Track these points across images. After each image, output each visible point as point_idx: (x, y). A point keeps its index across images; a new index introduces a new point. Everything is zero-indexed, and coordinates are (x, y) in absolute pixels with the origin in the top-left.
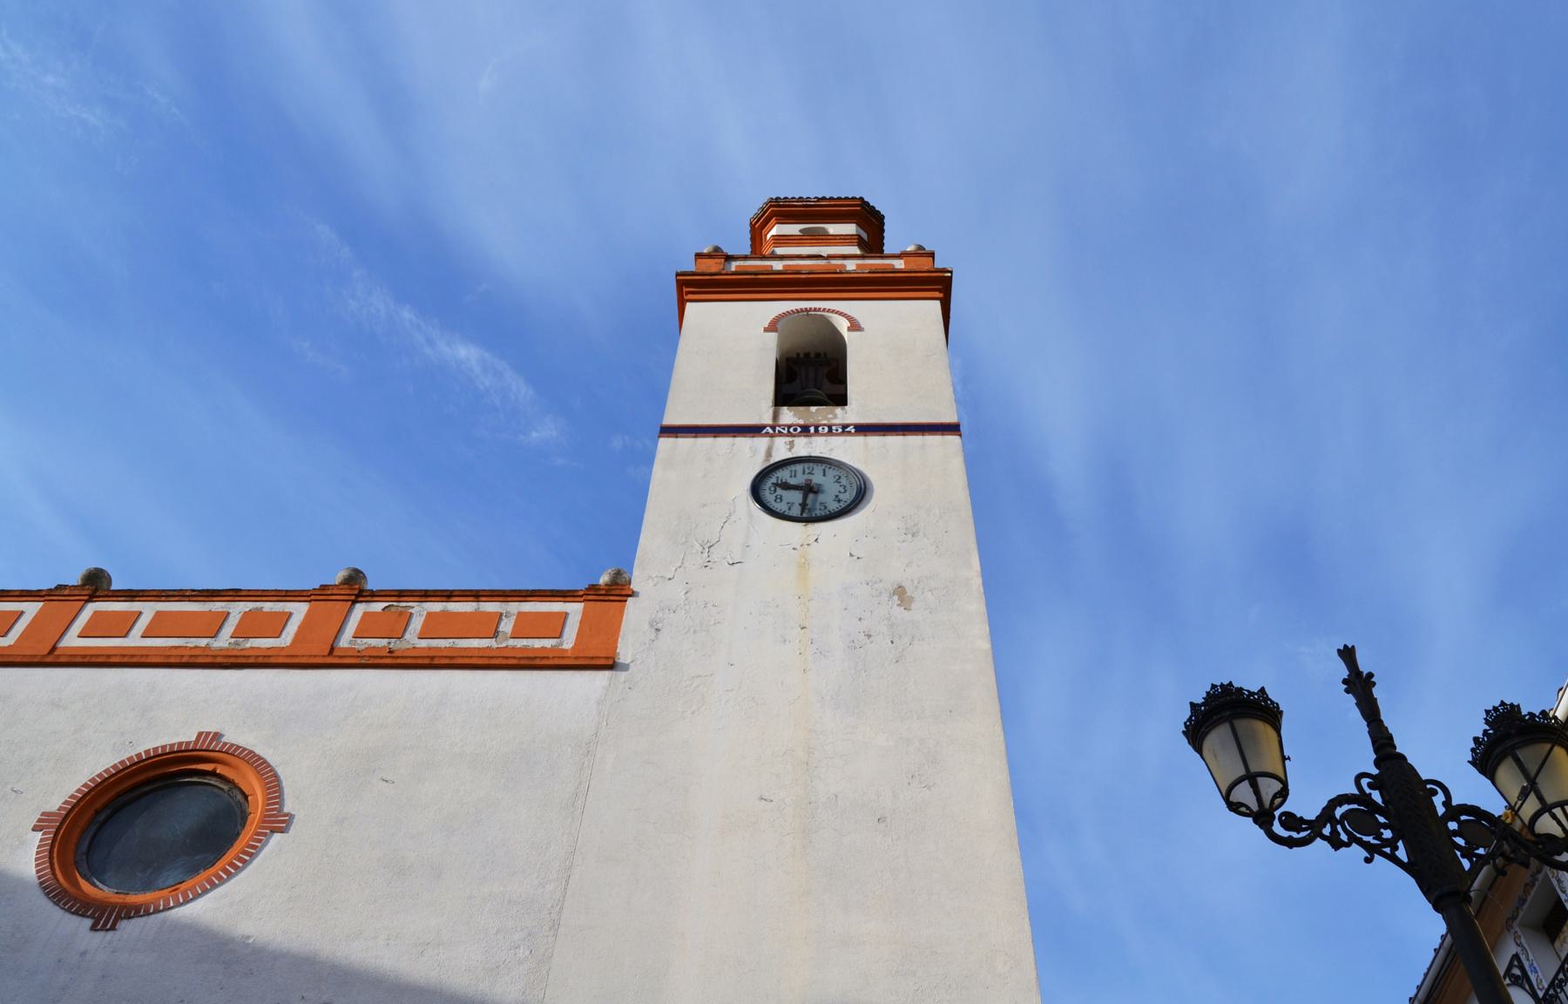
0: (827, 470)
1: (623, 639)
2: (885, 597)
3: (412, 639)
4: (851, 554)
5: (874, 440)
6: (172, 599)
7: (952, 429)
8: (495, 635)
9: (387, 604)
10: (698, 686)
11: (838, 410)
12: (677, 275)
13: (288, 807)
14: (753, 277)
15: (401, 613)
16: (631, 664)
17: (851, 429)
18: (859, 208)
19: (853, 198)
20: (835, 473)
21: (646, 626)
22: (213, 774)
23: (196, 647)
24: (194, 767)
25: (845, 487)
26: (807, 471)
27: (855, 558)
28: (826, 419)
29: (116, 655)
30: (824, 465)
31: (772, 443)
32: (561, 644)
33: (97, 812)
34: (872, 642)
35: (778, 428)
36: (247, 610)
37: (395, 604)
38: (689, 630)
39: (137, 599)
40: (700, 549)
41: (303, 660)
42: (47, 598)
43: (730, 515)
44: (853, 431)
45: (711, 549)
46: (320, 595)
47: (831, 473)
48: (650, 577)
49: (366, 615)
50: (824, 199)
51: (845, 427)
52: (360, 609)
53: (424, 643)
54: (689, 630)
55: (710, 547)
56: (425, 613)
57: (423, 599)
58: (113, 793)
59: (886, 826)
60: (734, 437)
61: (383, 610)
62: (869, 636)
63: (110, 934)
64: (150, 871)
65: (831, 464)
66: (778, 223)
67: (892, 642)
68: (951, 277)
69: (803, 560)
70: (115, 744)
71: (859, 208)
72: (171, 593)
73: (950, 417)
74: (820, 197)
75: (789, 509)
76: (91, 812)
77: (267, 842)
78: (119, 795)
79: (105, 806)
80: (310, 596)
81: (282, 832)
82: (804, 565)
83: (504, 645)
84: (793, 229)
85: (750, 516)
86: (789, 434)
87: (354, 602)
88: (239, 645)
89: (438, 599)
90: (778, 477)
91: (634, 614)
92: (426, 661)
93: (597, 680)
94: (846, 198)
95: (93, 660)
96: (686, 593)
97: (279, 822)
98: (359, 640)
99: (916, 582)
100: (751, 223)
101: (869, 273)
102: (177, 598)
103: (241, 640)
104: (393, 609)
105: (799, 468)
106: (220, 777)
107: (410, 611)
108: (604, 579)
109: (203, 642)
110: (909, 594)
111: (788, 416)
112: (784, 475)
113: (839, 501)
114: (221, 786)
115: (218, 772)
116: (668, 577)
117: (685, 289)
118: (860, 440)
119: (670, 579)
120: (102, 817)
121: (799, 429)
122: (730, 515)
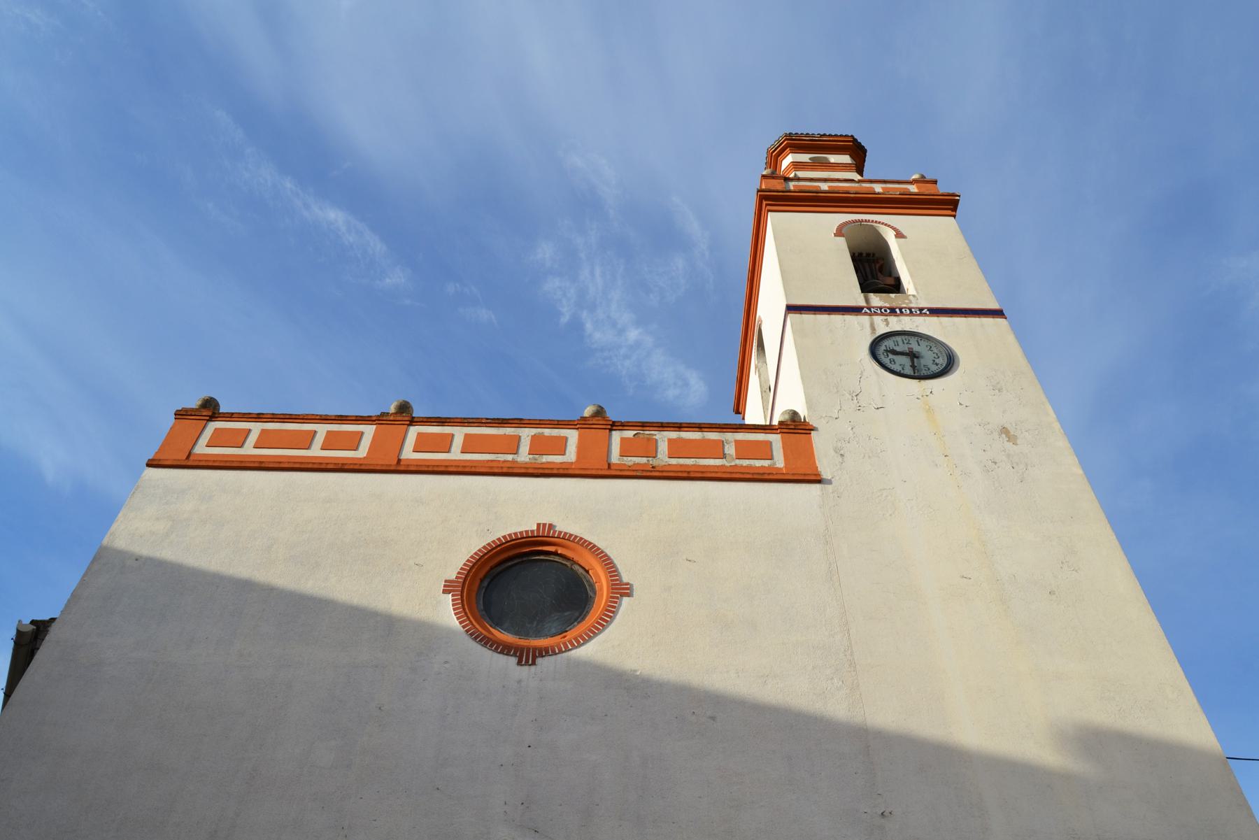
0: (919, 341)
1: (819, 462)
2: (996, 435)
3: (663, 457)
4: (960, 404)
6: (472, 425)
7: (997, 313)
8: (724, 456)
9: (636, 432)
10: (887, 496)
13: (625, 580)
15: (649, 440)
16: (833, 480)
19: (846, 136)
20: (927, 344)
21: (832, 453)
22: (556, 554)
23: (505, 461)
24: (540, 548)
25: (937, 354)
26: (905, 342)
28: (904, 303)
29: (452, 466)
33: (482, 581)
34: (999, 467)
35: (872, 309)
36: (533, 434)
38: (864, 456)
39: (447, 424)
41: (594, 472)
42: (377, 422)
44: (928, 313)
45: (858, 397)
47: (924, 343)
48: (821, 417)
50: (824, 135)
51: (921, 310)
53: (674, 461)
54: (864, 456)
55: (856, 396)
57: (661, 429)
58: (487, 568)
61: (634, 435)
62: (995, 463)
63: (533, 668)
64: (535, 623)
65: (921, 337)
66: (792, 153)
67: (1013, 468)
68: (959, 200)
69: (927, 407)
70: (477, 531)
72: (471, 421)
73: (994, 305)
74: (822, 134)
75: (903, 369)
76: (478, 581)
77: (620, 605)
78: (492, 568)
79: (485, 577)
81: (629, 596)
83: (733, 464)
84: (805, 158)
86: (882, 314)
87: (611, 430)
89: (672, 429)
90: (886, 346)
92: (685, 475)
94: (841, 136)
95: (436, 469)
98: (625, 458)
99: (1014, 425)
102: (476, 425)
103: (537, 456)
104: (641, 436)
105: (899, 339)
106: (561, 556)
107: (654, 437)
108: (588, 412)
109: (510, 457)
112: (889, 343)
113: (937, 364)
114: (563, 562)
115: (559, 552)
119: (836, 418)
120: (485, 584)
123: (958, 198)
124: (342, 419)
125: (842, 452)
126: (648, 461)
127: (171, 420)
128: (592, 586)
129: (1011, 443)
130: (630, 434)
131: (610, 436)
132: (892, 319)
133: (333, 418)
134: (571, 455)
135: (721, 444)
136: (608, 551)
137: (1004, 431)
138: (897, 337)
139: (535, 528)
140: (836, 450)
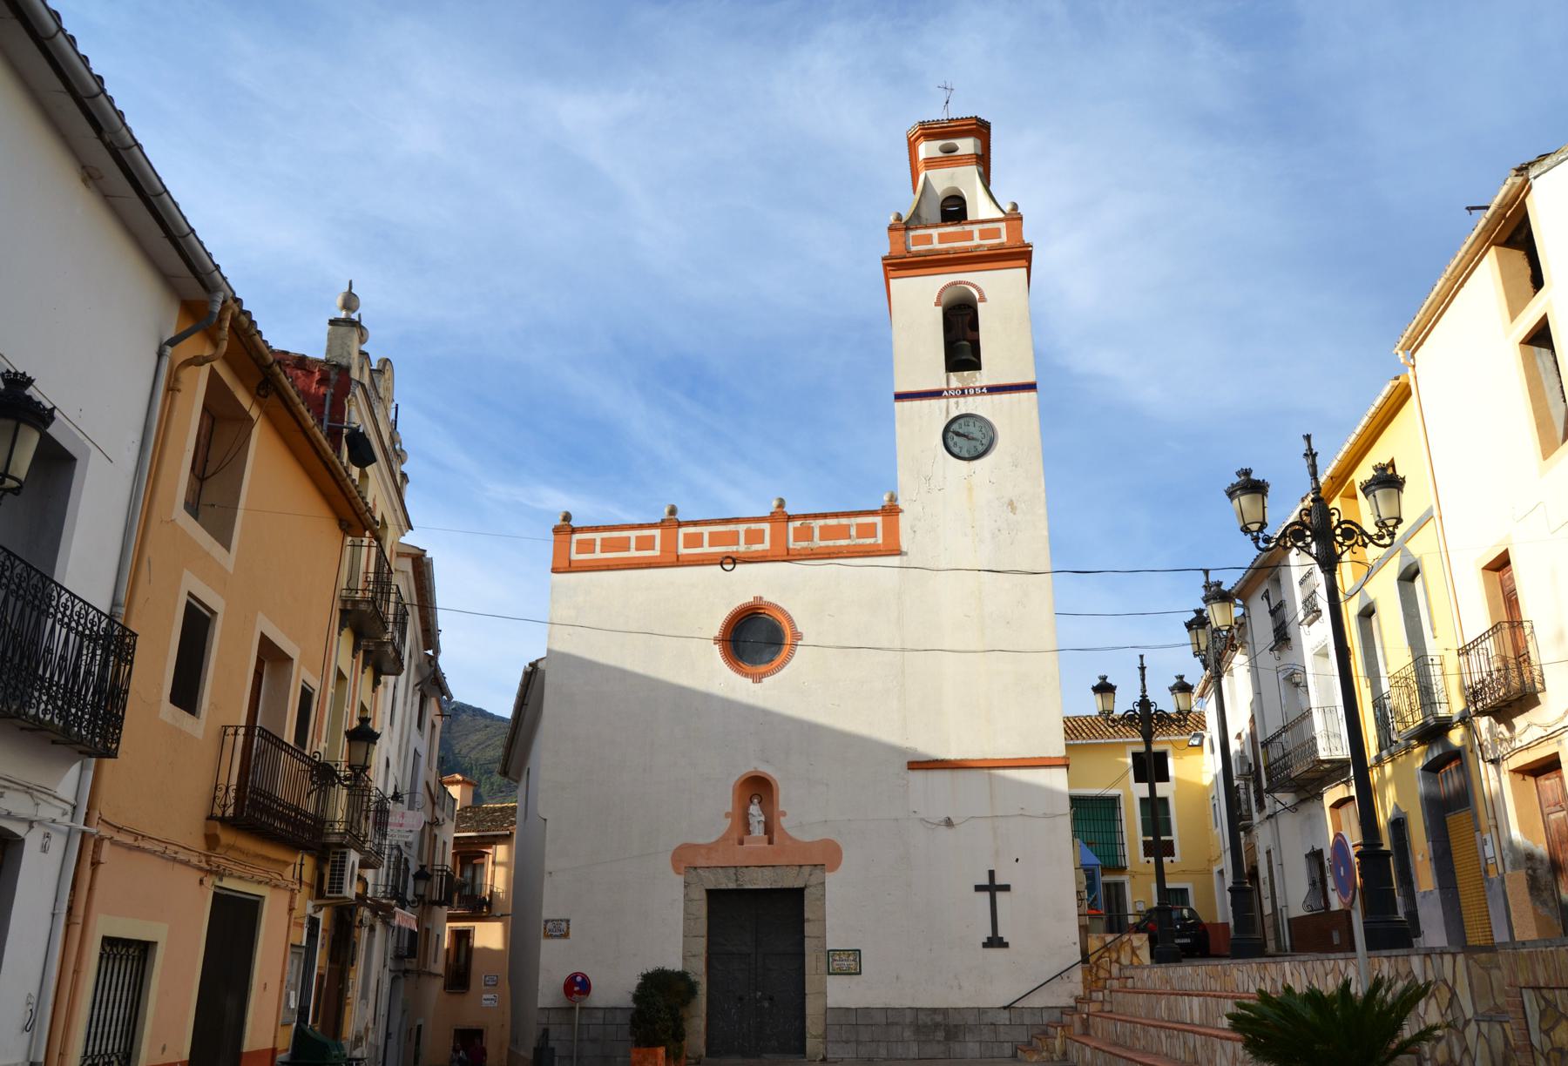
3: (818, 543)
5: (997, 397)
7: (1031, 387)
8: (850, 537)
11: (977, 373)
13: (799, 630)
17: (984, 390)
19: (971, 118)
21: (909, 531)
22: (764, 613)
31: (948, 402)
32: (877, 541)
46: (772, 518)
49: (795, 529)
50: (952, 119)
62: (999, 530)
63: (760, 684)
68: (1031, 251)
78: (737, 623)
82: (970, 489)
83: (854, 543)
86: (956, 396)
87: (787, 521)
91: (904, 520)
93: (895, 560)
97: (798, 636)
100: (909, 139)
106: (768, 615)
109: (734, 548)
111: (956, 380)
112: (955, 427)
117: (888, 268)
118: (989, 398)
123: (1030, 249)
124: (641, 526)
125: (915, 529)
127: (551, 536)
128: (783, 632)
130: (798, 523)
131: (787, 526)
132: (962, 400)
134: (766, 545)
135: (849, 527)
136: (790, 612)
137: (1011, 504)
139: (752, 600)
140: (912, 527)
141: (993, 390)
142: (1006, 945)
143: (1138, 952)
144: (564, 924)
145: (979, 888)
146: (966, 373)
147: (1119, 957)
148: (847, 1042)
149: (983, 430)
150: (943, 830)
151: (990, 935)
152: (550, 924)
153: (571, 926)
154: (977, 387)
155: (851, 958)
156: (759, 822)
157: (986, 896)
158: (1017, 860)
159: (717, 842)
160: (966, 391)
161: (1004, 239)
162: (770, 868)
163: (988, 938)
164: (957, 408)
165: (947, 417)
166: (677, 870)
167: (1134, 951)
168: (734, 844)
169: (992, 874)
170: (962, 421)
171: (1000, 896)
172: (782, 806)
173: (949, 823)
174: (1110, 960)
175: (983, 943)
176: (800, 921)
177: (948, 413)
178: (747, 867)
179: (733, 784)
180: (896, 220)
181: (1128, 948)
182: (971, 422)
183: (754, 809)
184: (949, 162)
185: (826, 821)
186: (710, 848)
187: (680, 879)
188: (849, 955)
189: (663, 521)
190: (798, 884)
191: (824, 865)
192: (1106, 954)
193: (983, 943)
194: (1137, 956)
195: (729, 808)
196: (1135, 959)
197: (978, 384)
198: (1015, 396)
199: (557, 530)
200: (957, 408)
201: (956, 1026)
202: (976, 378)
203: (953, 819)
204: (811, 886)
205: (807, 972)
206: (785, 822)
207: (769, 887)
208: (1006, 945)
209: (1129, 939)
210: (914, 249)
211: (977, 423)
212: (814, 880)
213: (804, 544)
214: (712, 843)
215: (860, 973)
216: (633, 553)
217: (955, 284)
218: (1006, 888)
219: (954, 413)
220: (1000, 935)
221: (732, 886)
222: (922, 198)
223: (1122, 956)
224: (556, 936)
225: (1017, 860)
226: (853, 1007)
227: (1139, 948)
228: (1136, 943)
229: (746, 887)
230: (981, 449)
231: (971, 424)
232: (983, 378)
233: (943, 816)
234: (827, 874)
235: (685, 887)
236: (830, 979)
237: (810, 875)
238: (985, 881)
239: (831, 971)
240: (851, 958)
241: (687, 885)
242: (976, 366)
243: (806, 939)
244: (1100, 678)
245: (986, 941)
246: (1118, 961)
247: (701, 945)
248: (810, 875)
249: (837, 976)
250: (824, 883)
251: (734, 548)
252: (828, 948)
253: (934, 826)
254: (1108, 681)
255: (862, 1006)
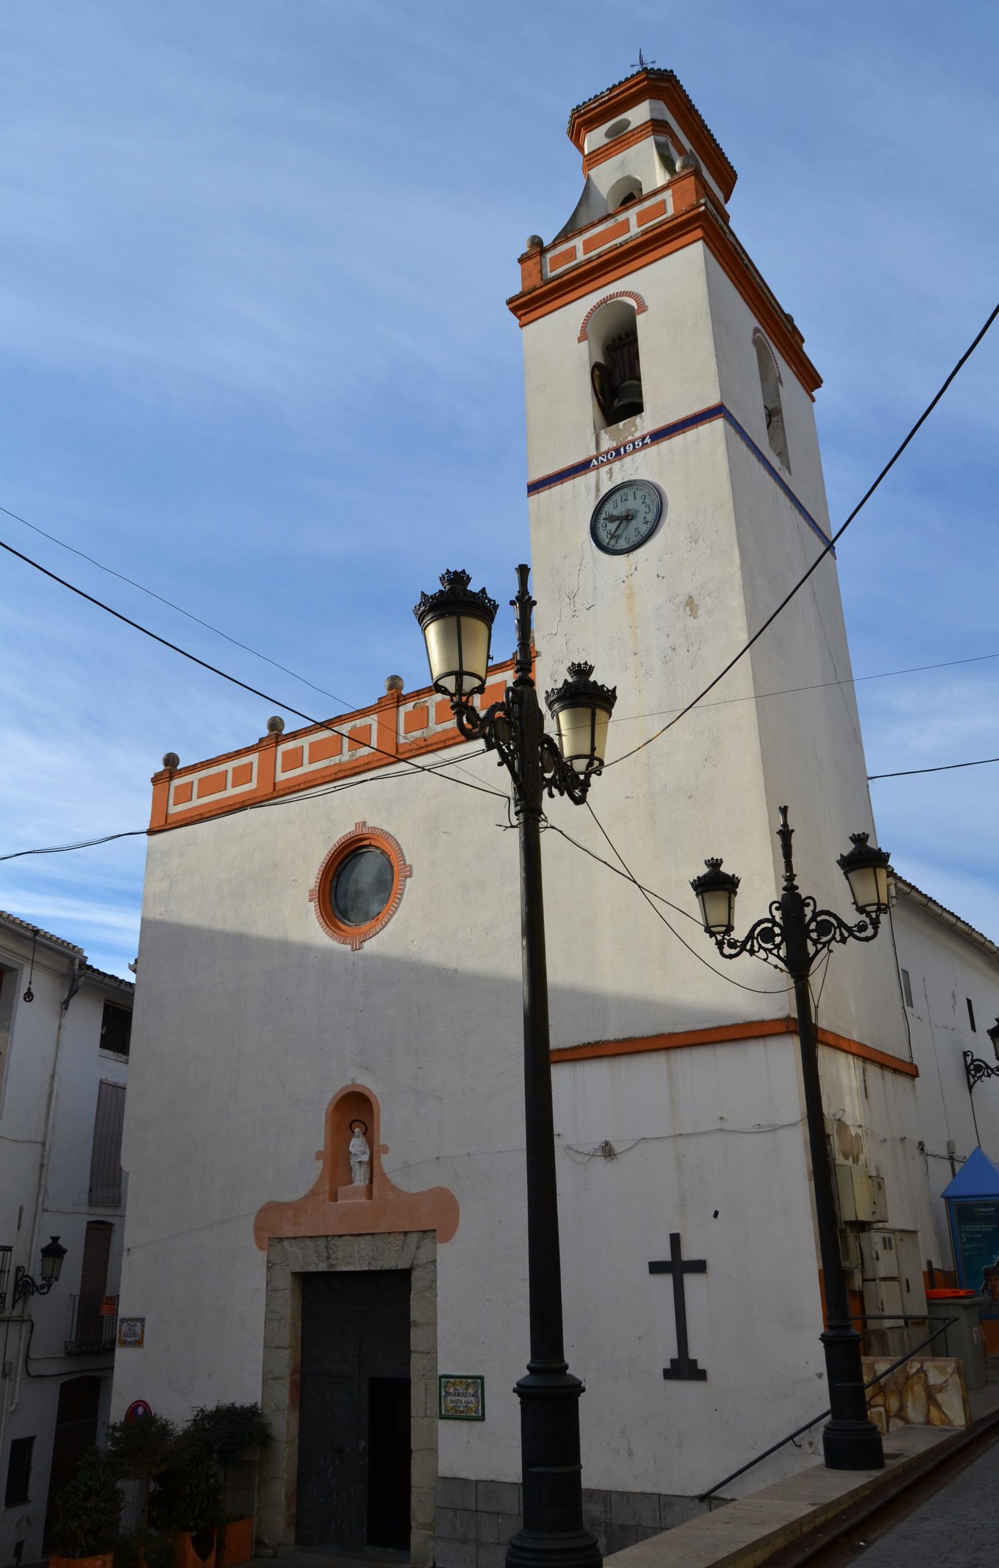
0: (636, 491)
5: (665, 445)
9: (414, 703)
11: (637, 419)
12: (508, 303)
14: (559, 281)
15: (423, 709)
17: (648, 440)
18: (645, 83)
22: (370, 845)
24: (361, 844)
27: (661, 577)
30: (634, 487)
31: (598, 475)
33: (331, 882)
34: (676, 654)
35: (600, 458)
36: (349, 729)
37: (418, 701)
40: (568, 601)
43: (582, 562)
45: (575, 599)
46: (379, 707)
48: (544, 636)
49: (406, 714)
52: (402, 710)
56: (434, 704)
58: (333, 870)
59: (693, 801)
60: (574, 478)
61: (413, 708)
62: (674, 649)
67: (688, 651)
69: (629, 590)
71: (645, 83)
76: (328, 883)
77: (405, 886)
78: (336, 869)
80: (375, 710)
82: (630, 596)
85: (594, 557)
86: (609, 462)
87: (398, 707)
88: (353, 756)
96: (566, 643)
99: (699, 589)
101: (642, 236)
103: (354, 751)
104: (418, 706)
107: (427, 704)
109: (337, 759)
110: (695, 603)
112: (609, 508)
113: (647, 523)
116: (554, 633)
117: (520, 313)
118: (653, 451)
119: (555, 634)
120: (334, 884)
121: (614, 454)
122: (582, 562)
126: (423, 733)
127: (150, 786)
129: (693, 617)
132: (616, 465)
133: (233, 755)
138: (614, 496)
141: (659, 435)
142: (701, 1375)
143: (939, 1397)
144: (139, 1324)
145: (656, 1268)
146: (621, 424)
147: (902, 1407)
148: (463, 1541)
149: (648, 501)
150: (600, 1162)
151: (676, 1356)
152: (125, 1324)
153: (146, 1329)
154: (637, 439)
155: (471, 1391)
156: (360, 1162)
157: (666, 1281)
158: (716, 1214)
159: (306, 1197)
160: (622, 450)
161: (670, 211)
162: (367, 1238)
163: (672, 1361)
164: (610, 478)
165: (597, 496)
166: (262, 1248)
167: (931, 1395)
168: (324, 1201)
169: (675, 1240)
170: (617, 496)
171: (691, 1281)
172: (384, 1136)
173: (608, 1151)
174: (886, 1411)
175: (665, 1371)
176: (403, 1324)
177: (598, 490)
178: (341, 1236)
179: (325, 1107)
180: (530, 247)
181: (919, 1389)
182: (630, 492)
183: (357, 1145)
184: (617, 147)
185: (438, 1158)
186: (297, 1207)
187: (262, 1256)
188: (468, 1385)
189: (261, 740)
190: (403, 1264)
191: (435, 1230)
192: (879, 1400)
193: (665, 1371)
194: (938, 1406)
195: (321, 1147)
196: (934, 1413)
197: (638, 434)
198: (691, 434)
199: (156, 780)
200: (610, 478)
201: (623, 1527)
202: (636, 427)
203: (614, 1145)
204: (419, 1266)
205: (413, 1414)
206: (387, 1163)
207: (366, 1268)
208: (701, 1375)
209: (921, 1370)
210: (551, 275)
211: (639, 494)
212: (422, 1258)
213: (417, 734)
214: (300, 1200)
215: (482, 1418)
216: (231, 792)
217: (604, 301)
218: (699, 1267)
219: (606, 488)
220: (692, 1356)
221: (322, 1267)
222: (583, 209)
223: (910, 1405)
224: (130, 1343)
225: (716, 1214)
226: (473, 1478)
227: (941, 1388)
228: (935, 1378)
229: (339, 1269)
230: (644, 529)
231: (631, 496)
232: (646, 423)
233: (598, 1141)
234: (439, 1245)
235: (269, 1269)
236: (443, 1425)
237: (418, 1248)
238: (665, 1254)
239: (443, 1412)
240: (471, 1391)
241: (270, 1266)
242: (637, 408)
243: (413, 1356)
244: (708, 863)
245: (668, 1366)
246: (901, 1414)
247: (285, 1361)
248: (418, 1248)
249: (452, 1423)
250: (434, 1261)
251: (337, 759)
252: (440, 1373)
253: (587, 1158)
254: (723, 869)
255: (484, 1478)
